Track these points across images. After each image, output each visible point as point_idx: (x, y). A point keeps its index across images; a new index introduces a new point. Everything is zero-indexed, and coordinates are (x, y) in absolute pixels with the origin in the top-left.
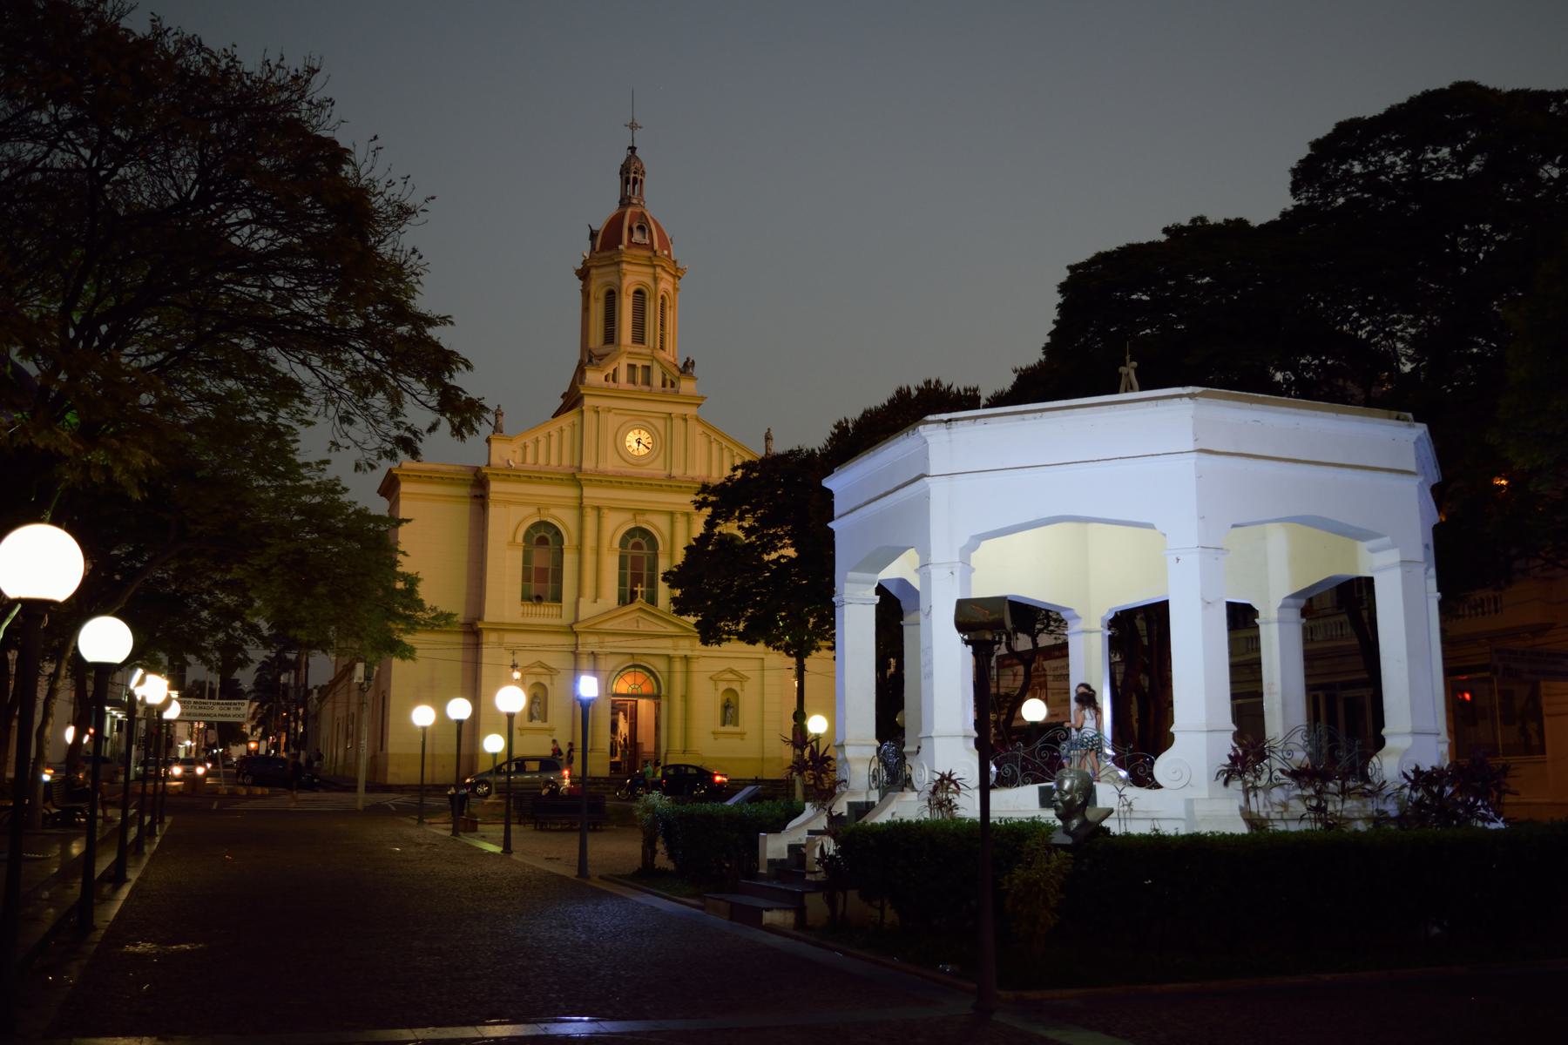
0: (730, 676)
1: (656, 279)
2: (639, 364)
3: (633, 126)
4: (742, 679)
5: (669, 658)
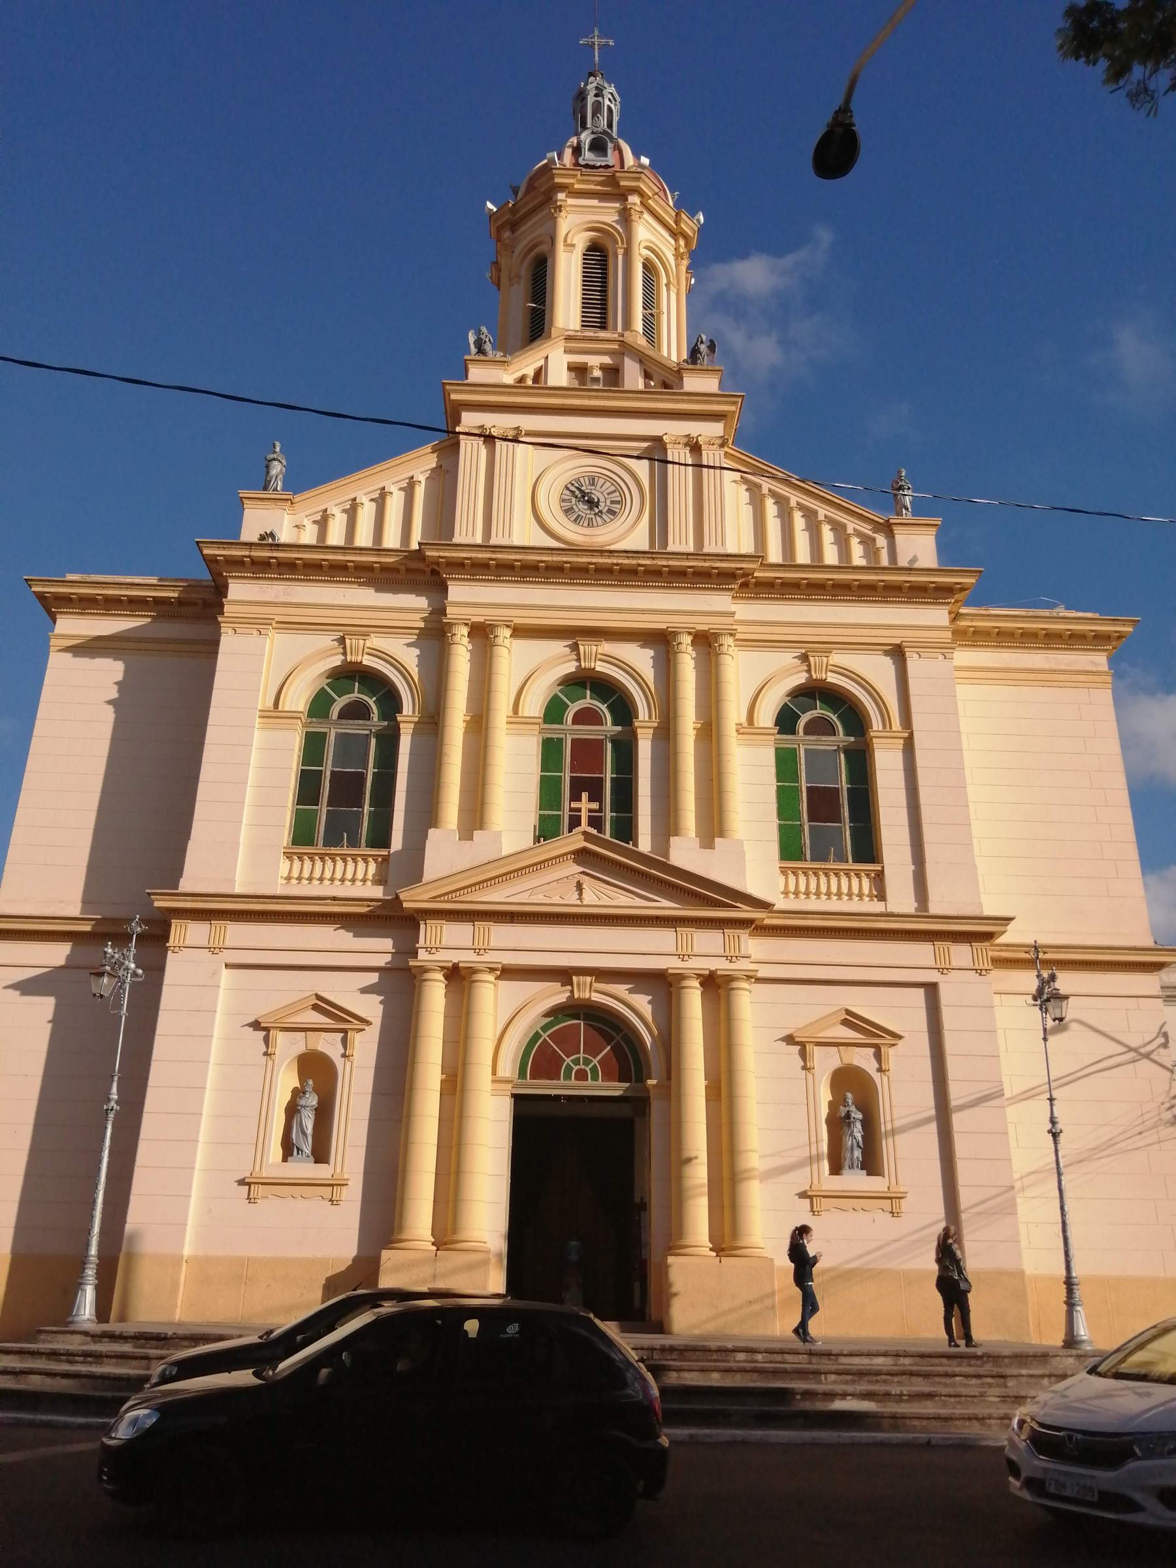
1: (625, 217)
2: (594, 361)
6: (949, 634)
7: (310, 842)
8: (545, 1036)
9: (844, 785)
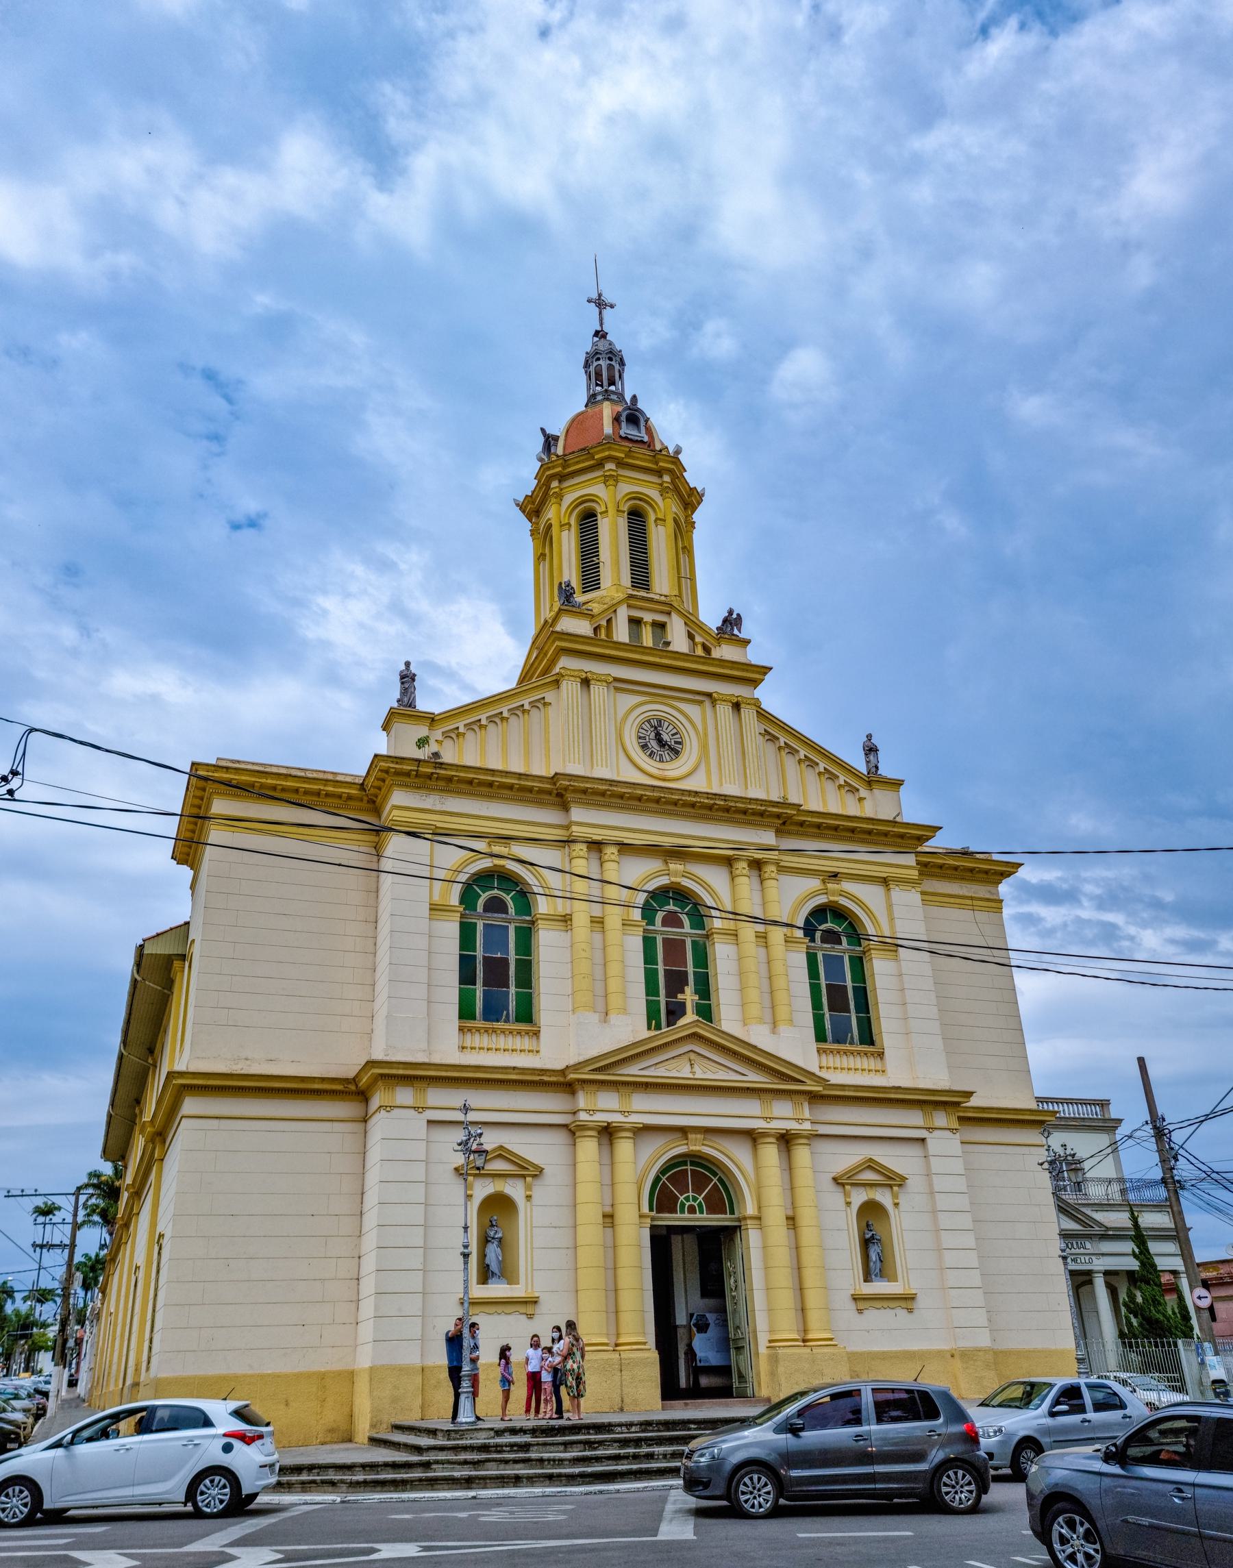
0: (869, 1176)
2: (648, 617)
4: (893, 1181)
5: (752, 1137)
6: (916, 873)
7: (473, 1017)
8: (664, 1179)
9: (849, 984)
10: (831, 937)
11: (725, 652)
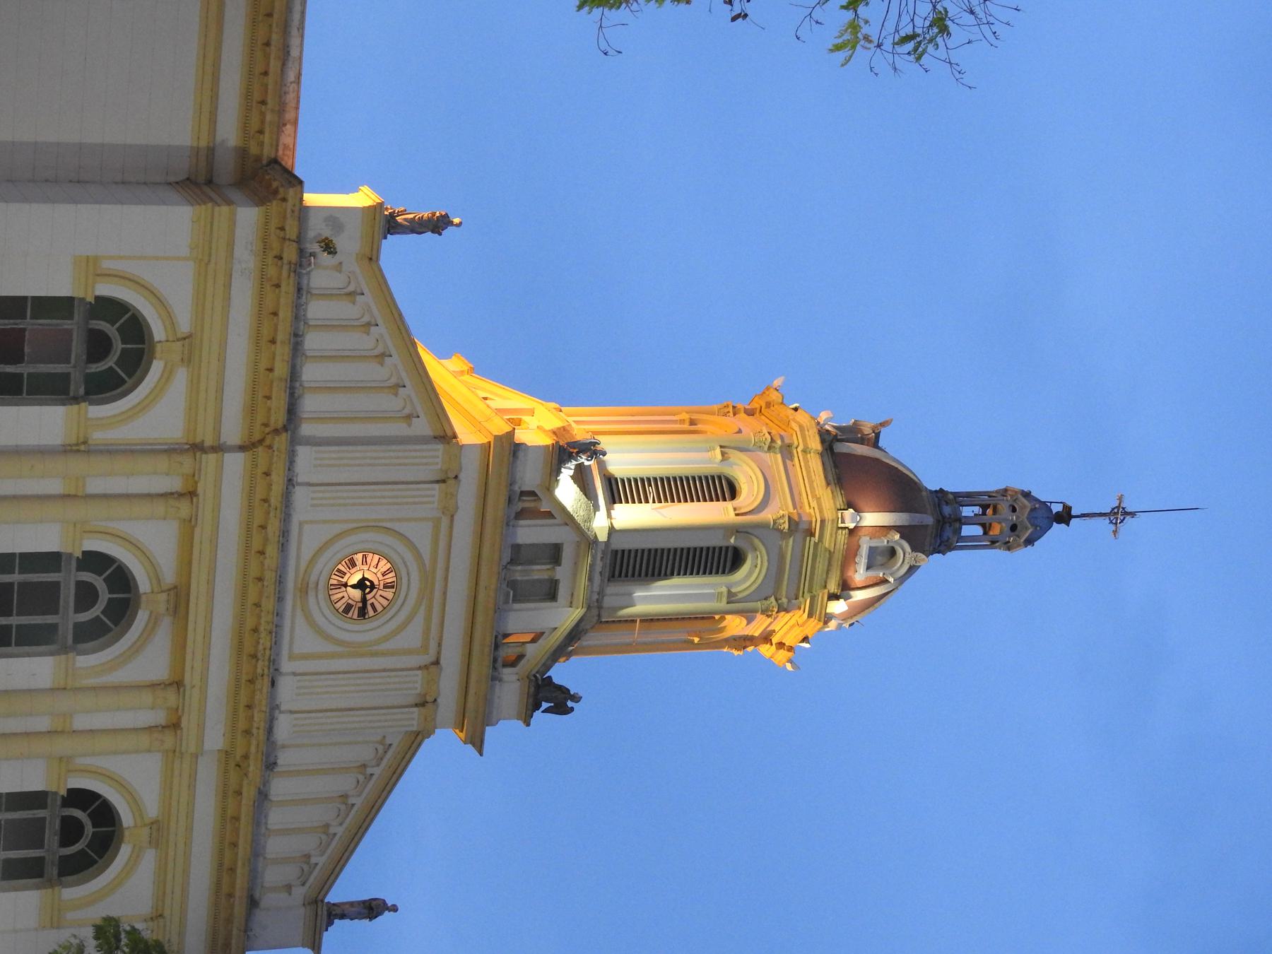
2: (562, 573)
3: (1118, 514)
10: (70, 831)
11: (511, 688)
